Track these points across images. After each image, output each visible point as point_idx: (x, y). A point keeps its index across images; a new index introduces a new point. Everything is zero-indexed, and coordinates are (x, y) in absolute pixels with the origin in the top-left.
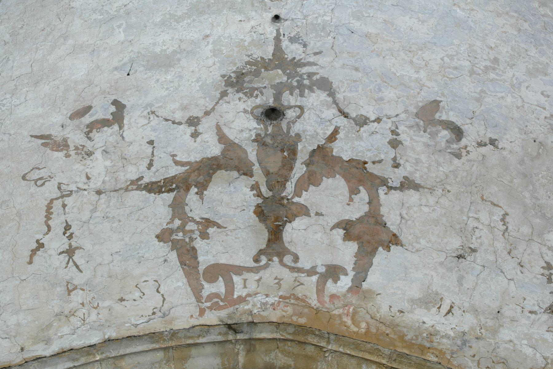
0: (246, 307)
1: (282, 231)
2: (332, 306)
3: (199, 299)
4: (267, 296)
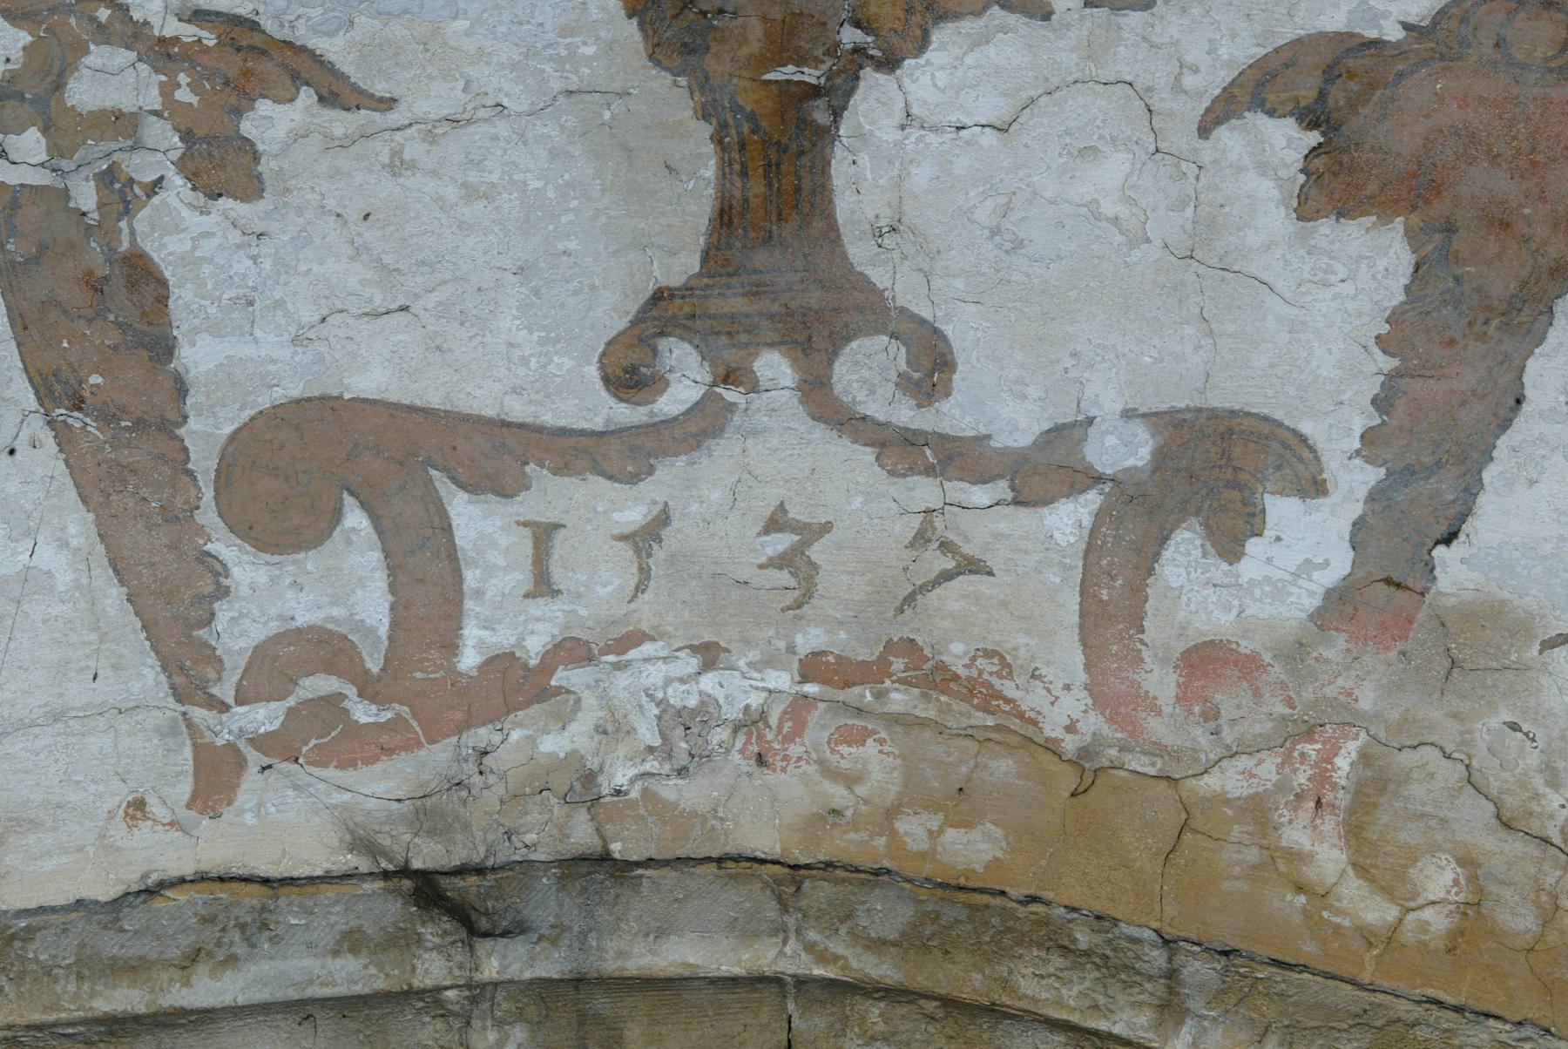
0: (553, 744)
1: (825, 136)
2: (1201, 736)
4: (710, 656)
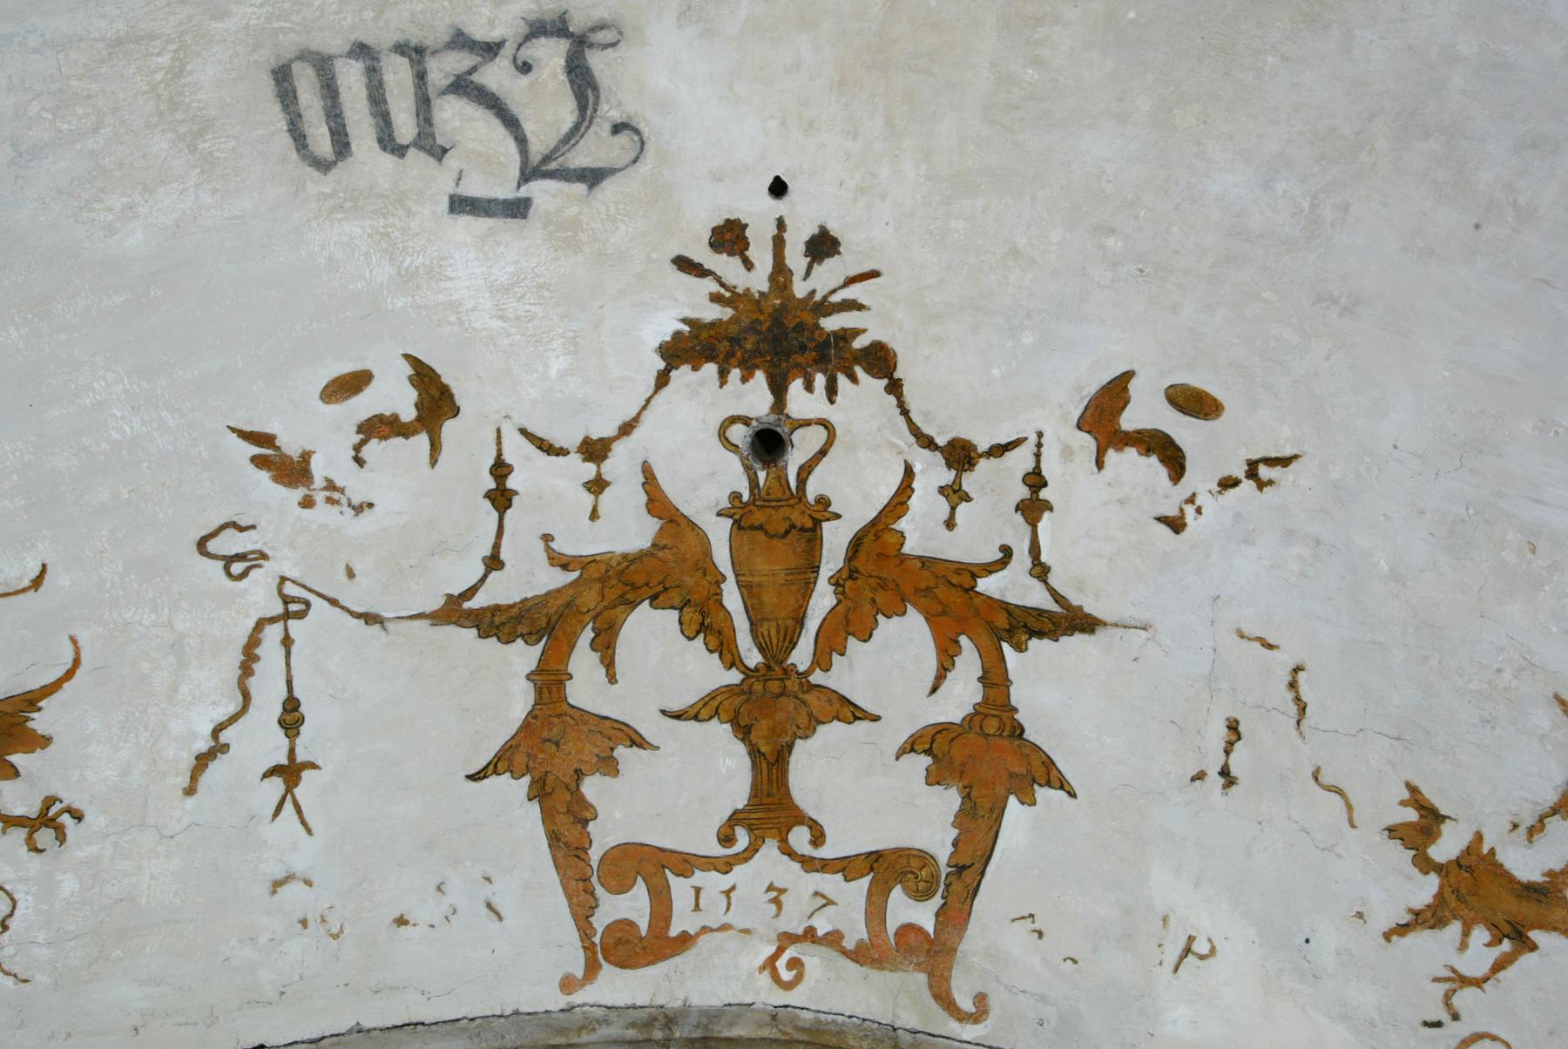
3: (584, 928)
